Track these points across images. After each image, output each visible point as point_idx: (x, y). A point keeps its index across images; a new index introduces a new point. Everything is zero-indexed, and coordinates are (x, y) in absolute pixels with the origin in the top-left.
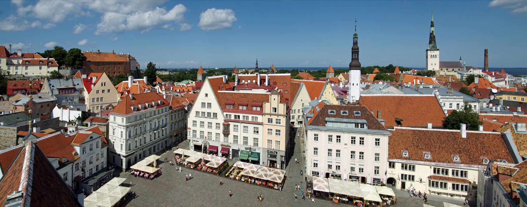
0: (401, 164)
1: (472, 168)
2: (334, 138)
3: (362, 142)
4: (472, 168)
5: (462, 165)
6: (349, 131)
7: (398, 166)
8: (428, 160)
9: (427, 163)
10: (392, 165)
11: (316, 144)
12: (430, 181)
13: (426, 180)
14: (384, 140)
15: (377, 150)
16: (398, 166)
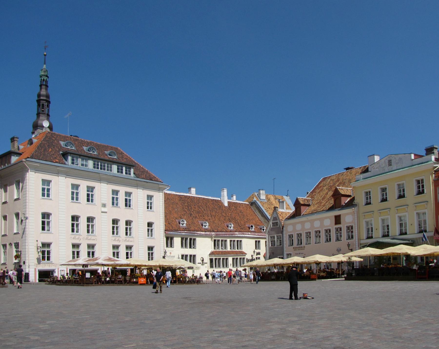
0: (179, 239)
1: (246, 235)
2: (83, 193)
3: (128, 204)
4: (246, 235)
5: (237, 233)
6: (110, 180)
7: (177, 241)
8: (206, 230)
9: (208, 233)
10: (169, 241)
11: (46, 206)
12: (211, 260)
13: (207, 260)
14: (159, 199)
15: (151, 217)
16: (177, 241)
